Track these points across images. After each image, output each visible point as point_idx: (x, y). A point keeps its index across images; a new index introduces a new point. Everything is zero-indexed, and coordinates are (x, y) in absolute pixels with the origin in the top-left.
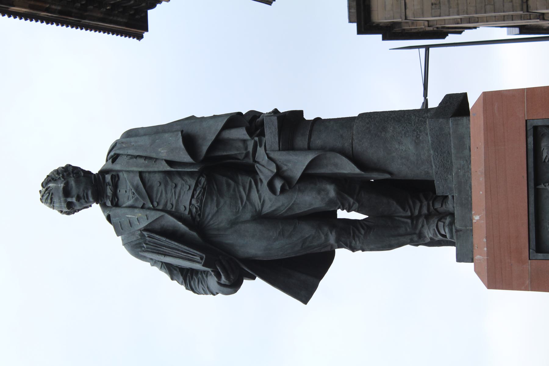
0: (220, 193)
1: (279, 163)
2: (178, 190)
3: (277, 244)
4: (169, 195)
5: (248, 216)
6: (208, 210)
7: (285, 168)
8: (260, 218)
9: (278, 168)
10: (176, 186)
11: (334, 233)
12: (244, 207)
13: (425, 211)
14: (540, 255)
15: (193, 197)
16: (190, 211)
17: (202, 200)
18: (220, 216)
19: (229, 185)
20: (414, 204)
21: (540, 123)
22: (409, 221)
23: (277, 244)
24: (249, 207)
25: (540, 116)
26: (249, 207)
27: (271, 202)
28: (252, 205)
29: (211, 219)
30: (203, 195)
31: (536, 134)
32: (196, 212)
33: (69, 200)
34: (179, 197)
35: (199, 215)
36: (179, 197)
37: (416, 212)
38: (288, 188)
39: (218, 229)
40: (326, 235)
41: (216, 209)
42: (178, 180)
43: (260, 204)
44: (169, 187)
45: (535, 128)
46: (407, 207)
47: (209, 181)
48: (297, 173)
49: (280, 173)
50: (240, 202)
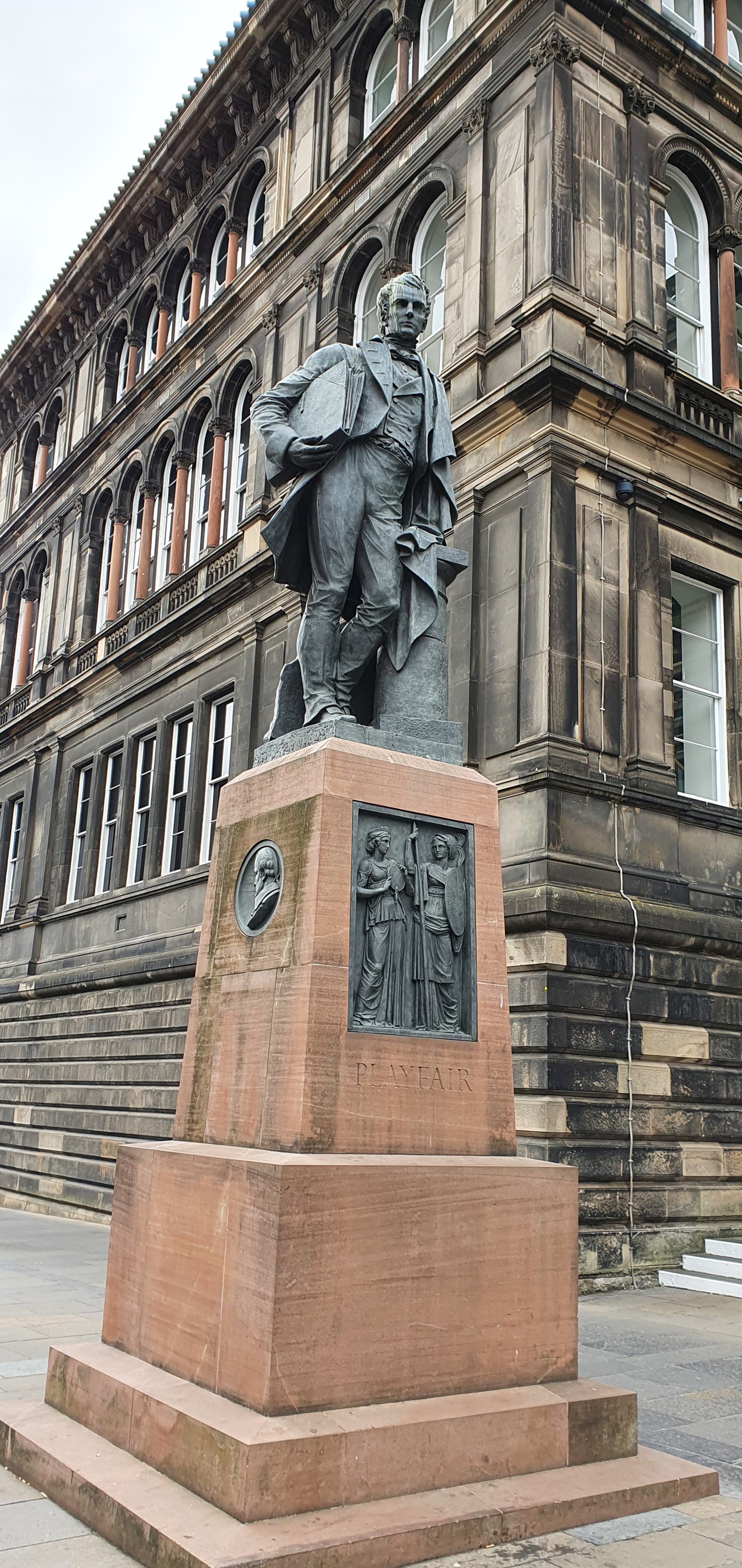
0: (397, 478)
1: (425, 553)
2: (406, 431)
3: (340, 522)
4: (403, 419)
5: (372, 499)
6: (385, 457)
7: (421, 558)
8: (367, 512)
9: (423, 550)
10: (410, 430)
11: (342, 590)
12: (381, 499)
13: (341, 696)
14: (356, 813)
15: (401, 445)
16: (387, 437)
17: (396, 454)
18: (376, 467)
19: (399, 489)
20: (348, 687)
21: (470, 837)
22: (334, 677)
23: (340, 522)
24: (381, 505)
25: (477, 839)
26: (381, 505)
27: (387, 530)
28: (381, 510)
29: (375, 458)
30: (400, 458)
31: (461, 832)
32: (386, 443)
33: (410, 305)
34: (400, 430)
35: (380, 445)
36: (400, 430)
37: (339, 686)
38: (402, 554)
39: (361, 461)
40: (340, 581)
41: (385, 467)
42: (412, 436)
43: (382, 518)
44: (409, 423)
45: (465, 832)
46: (347, 679)
47: (408, 468)
48: (416, 567)
49: (419, 551)
50: (386, 496)
